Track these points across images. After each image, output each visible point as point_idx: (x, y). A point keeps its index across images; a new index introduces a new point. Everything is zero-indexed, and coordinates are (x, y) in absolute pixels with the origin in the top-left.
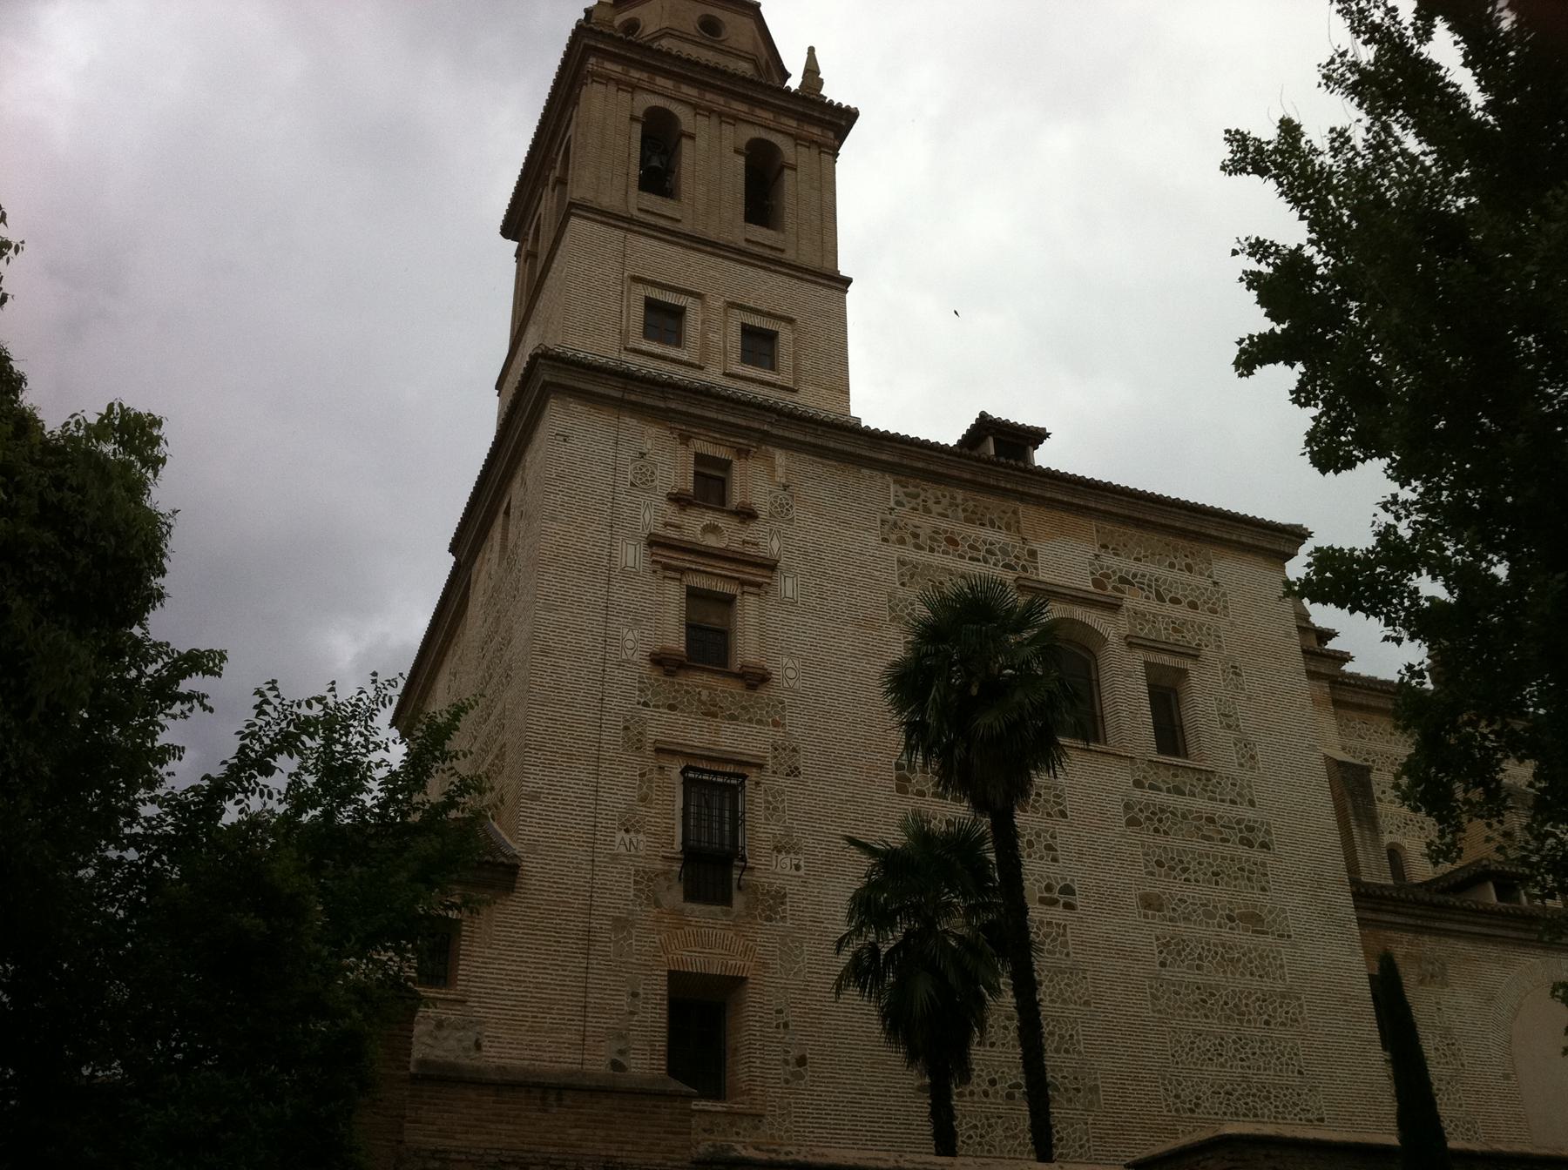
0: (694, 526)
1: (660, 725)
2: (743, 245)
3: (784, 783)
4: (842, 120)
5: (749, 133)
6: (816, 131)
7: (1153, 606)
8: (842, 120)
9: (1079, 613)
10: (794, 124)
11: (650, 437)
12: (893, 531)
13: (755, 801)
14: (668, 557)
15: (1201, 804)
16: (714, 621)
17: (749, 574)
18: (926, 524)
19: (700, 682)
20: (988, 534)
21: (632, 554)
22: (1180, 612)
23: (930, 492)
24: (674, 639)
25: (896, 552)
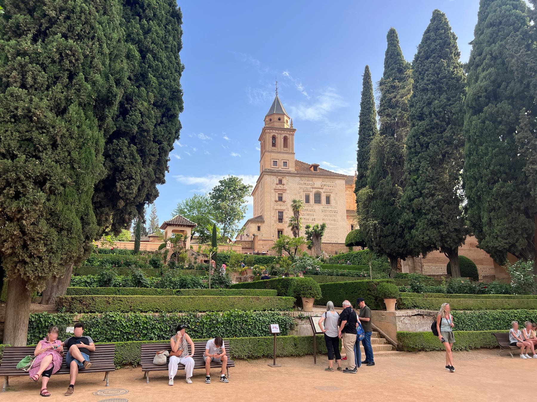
0: (279, 187)
1: (276, 207)
2: (283, 151)
3: (287, 211)
4: (295, 130)
5: (284, 135)
6: (291, 133)
7: (328, 188)
8: (295, 130)
9: (319, 190)
10: (289, 132)
11: (274, 178)
12: (299, 184)
13: (284, 213)
14: (276, 190)
15: (330, 209)
16: (281, 196)
17: (284, 191)
18: (302, 182)
19: (280, 203)
20: (309, 182)
21: (273, 191)
22: (331, 188)
23: (303, 178)
24: (277, 199)
25: (299, 186)
